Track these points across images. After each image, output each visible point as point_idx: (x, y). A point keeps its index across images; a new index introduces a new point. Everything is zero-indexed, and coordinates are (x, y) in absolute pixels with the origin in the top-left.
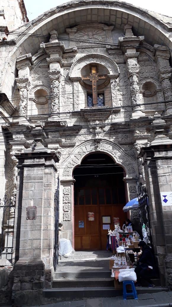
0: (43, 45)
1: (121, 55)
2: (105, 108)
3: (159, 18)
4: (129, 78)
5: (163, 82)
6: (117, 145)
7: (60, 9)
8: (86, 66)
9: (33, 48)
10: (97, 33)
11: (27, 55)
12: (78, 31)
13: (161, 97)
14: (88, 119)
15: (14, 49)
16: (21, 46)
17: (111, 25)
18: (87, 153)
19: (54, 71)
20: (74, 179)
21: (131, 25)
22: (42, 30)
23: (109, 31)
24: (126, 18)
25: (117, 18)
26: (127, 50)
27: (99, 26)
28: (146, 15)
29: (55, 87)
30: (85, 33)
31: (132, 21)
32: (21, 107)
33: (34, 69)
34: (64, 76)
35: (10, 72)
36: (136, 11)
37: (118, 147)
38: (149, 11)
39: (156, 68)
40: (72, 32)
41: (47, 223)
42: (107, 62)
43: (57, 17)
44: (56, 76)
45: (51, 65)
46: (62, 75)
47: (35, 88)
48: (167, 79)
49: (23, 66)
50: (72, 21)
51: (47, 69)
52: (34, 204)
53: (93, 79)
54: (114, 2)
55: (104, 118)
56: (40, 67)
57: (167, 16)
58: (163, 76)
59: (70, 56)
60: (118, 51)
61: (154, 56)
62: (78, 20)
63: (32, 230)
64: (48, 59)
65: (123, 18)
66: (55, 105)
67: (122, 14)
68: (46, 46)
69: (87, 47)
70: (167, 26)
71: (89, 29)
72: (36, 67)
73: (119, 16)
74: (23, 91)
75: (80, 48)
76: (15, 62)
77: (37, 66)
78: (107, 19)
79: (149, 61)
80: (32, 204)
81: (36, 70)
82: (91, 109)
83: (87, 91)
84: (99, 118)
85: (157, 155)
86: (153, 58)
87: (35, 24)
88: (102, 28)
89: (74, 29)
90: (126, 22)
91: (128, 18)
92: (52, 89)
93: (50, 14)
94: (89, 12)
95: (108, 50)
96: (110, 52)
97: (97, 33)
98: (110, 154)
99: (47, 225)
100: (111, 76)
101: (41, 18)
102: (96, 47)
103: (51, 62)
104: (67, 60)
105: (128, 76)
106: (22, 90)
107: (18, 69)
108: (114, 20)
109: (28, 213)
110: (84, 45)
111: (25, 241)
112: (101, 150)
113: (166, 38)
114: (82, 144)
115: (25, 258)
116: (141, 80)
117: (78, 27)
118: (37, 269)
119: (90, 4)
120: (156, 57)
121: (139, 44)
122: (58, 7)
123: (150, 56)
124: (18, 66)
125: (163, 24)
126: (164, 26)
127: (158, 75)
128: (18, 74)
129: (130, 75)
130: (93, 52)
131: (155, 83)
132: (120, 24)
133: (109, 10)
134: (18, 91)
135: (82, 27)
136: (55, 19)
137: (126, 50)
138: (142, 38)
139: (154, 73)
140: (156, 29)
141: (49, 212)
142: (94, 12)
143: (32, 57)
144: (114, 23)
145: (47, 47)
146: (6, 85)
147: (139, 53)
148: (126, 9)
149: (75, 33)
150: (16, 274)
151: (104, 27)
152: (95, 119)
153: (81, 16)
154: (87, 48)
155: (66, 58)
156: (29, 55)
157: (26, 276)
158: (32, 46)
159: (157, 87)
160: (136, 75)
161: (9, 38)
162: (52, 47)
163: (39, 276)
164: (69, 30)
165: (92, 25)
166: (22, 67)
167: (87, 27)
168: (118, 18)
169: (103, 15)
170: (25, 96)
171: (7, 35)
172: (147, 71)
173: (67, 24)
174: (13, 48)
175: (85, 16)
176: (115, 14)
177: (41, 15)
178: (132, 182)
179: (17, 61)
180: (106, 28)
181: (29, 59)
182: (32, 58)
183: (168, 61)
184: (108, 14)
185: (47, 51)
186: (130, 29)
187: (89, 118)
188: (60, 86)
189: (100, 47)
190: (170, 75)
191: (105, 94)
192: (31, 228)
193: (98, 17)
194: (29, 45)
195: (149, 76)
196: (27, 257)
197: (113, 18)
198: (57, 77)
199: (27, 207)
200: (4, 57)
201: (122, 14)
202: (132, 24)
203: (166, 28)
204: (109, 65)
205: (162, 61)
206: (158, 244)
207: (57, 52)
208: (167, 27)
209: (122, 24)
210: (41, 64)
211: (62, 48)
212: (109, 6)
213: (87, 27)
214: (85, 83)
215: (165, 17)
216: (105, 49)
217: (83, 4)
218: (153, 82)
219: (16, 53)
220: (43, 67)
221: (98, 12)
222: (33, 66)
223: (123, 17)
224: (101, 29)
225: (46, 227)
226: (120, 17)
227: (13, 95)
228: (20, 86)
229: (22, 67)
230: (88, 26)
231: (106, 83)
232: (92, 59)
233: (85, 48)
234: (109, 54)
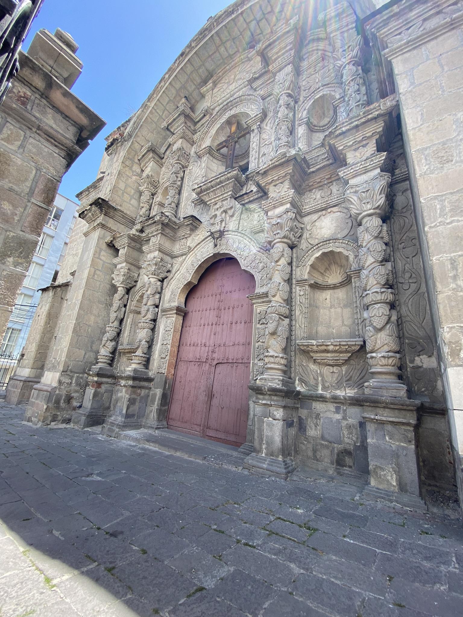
22: (163, 105)
40: (208, 91)
49: (148, 162)
76: (136, 161)
84: (221, 197)
89: (210, 85)
93: (167, 76)
96: (255, 85)
102: (237, 92)
117: (215, 78)
135: (220, 74)
149: (213, 90)
152: (216, 200)
153: (210, 56)
162: (174, 120)
164: (204, 89)
167: (227, 71)
193: (234, 43)
222: (164, 160)
224: (246, 61)
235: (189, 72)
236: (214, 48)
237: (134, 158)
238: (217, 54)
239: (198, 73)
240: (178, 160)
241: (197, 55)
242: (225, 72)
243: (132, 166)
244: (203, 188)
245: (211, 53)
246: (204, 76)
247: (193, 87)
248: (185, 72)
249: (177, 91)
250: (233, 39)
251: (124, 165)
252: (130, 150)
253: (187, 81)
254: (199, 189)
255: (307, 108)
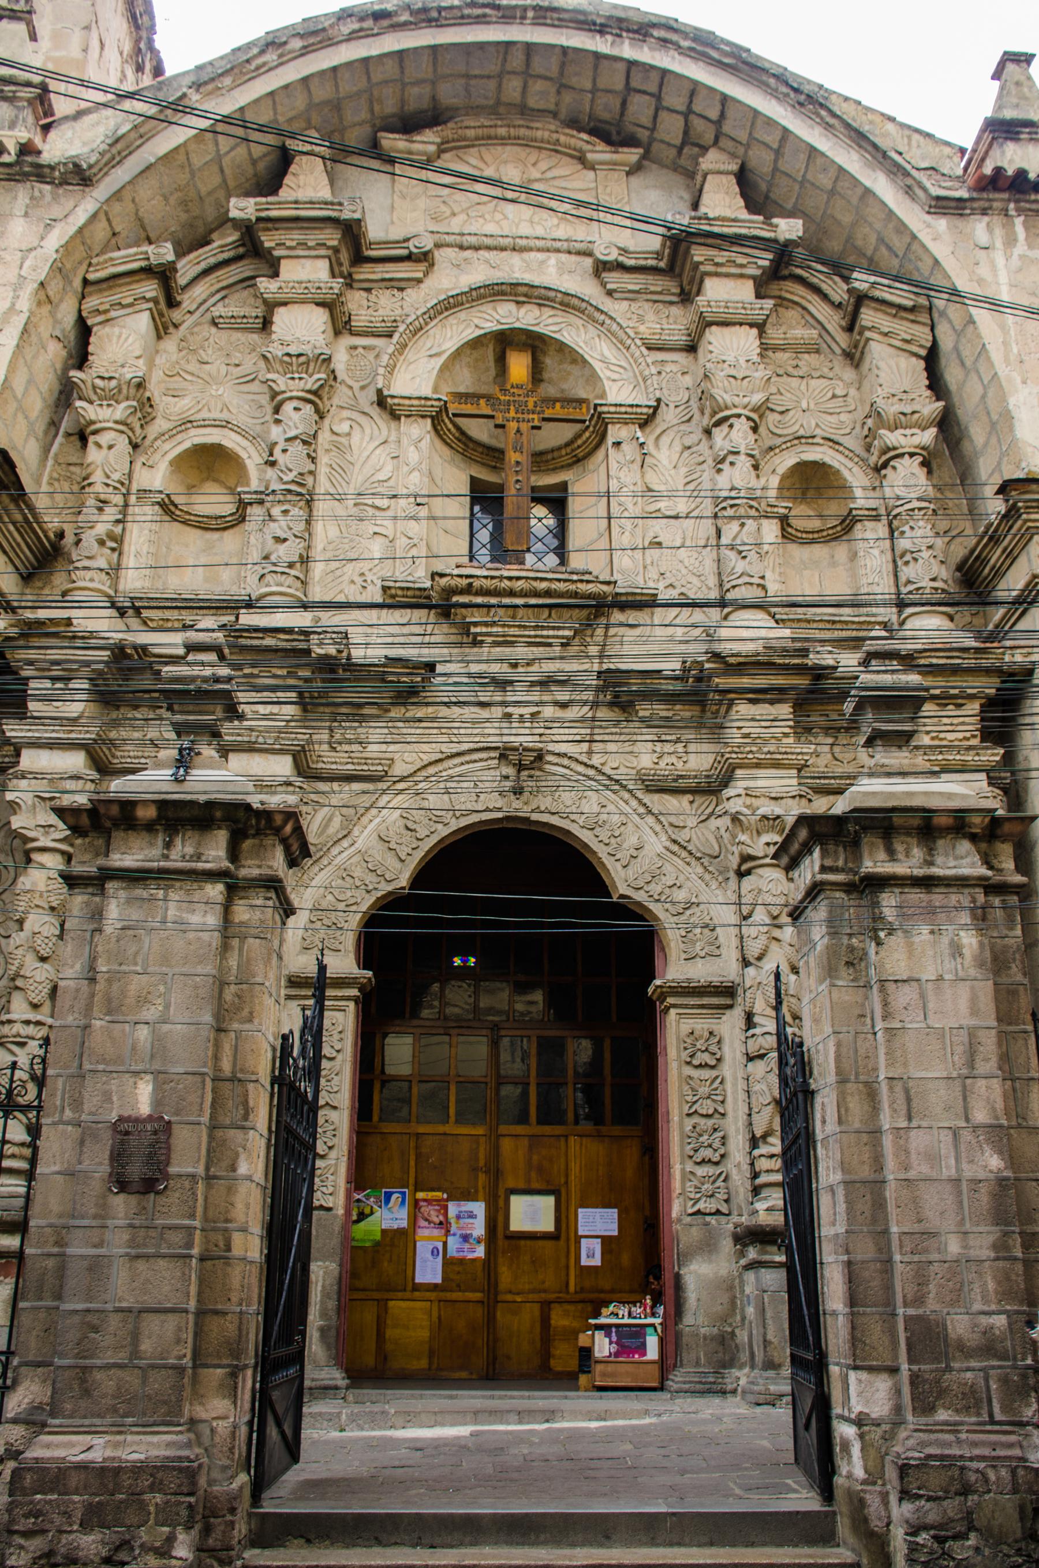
0: (244, 208)
1: (671, 303)
2: (575, 577)
3: (888, 138)
4: (708, 432)
5: (888, 471)
6: (630, 791)
7: (356, 26)
8: (475, 344)
9: (184, 216)
10: (549, 175)
11: (150, 249)
12: (444, 151)
13: (876, 552)
14: (473, 630)
15: (83, 207)
16: (117, 195)
17: (630, 141)
18: (455, 825)
19: (293, 350)
20: (369, 974)
21: (733, 155)
23: (616, 174)
24: (714, 114)
25: (663, 115)
26: (709, 283)
27: (563, 139)
28: (818, 115)
29: (296, 438)
30: (481, 165)
31: (743, 136)
32: (89, 539)
33: (182, 328)
34: (350, 382)
35: (46, 335)
36: (768, 85)
37: (634, 803)
38: (833, 98)
39: (853, 392)
41: (227, 1221)
42: (592, 331)
43: (335, 63)
44: (310, 383)
45: (282, 317)
46: (341, 375)
47: (179, 438)
48: (912, 455)
49: (124, 307)
50: (417, 98)
51: (255, 336)
52: (157, 1102)
53: (512, 414)
54: (654, 26)
55: (561, 633)
56: (216, 324)
57: (928, 136)
58: (892, 438)
59: (391, 280)
60: (657, 283)
61: (850, 328)
62: (449, 94)
63: (138, 1257)
64: (265, 285)
65: (692, 117)
66: (285, 540)
67: (692, 94)
68: (263, 214)
69: (488, 241)
70: (928, 184)
71: (509, 151)
72: (190, 320)
73: (675, 100)
74: (110, 447)
75: (448, 245)
76: (77, 283)
77: (198, 314)
78: (606, 108)
79: (818, 351)
80: (143, 1098)
81: (190, 338)
82: (493, 578)
83: (474, 482)
85: (875, 862)
86: (843, 339)
87: (210, 87)
88: (580, 151)
89: (426, 141)
90: (709, 137)
91: (722, 115)
92: (277, 451)
93: (297, 44)
94: (517, 61)
95: (601, 268)
96: (615, 280)
97: (549, 175)
98: (585, 836)
99: (226, 1230)
100: (612, 409)
101: (248, 61)
102: (539, 250)
103: (285, 304)
104: (372, 298)
105: (706, 421)
106: (104, 439)
107: (89, 322)
108: (646, 120)
109: (118, 1157)
110: (473, 229)
111: (89, 1318)
112: (535, 817)
113: (915, 247)
114: (424, 767)
115: (87, 1422)
116: (771, 449)
117: (448, 131)
118: (152, 1489)
119: (523, 17)
120: (861, 334)
121: (771, 256)
122: (345, 15)
123: (829, 327)
124: (92, 302)
125: (907, 174)
126: (909, 181)
127: (866, 432)
128: (91, 349)
129: (715, 413)
130: (516, 269)
131: (846, 473)
132: (678, 142)
133: (621, 67)
134: (78, 444)
136: (322, 73)
137: (702, 282)
138: (789, 228)
139: (843, 417)
140: (868, 192)
141: (243, 1157)
142: (538, 66)
143: (179, 266)
144: (643, 135)
145: (268, 220)
146: (15, 405)
147: (769, 304)
148: (713, 69)
150: (26, 1516)
151: (589, 147)
153: (468, 76)
154: (489, 248)
155: (368, 290)
156: (166, 252)
157: (86, 1526)
158: (184, 203)
159: (858, 493)
160: (749, 418)
161: (57, 148)
162: (297, 219)
163: (166, 1529)
164: (393, 142)
165: (522, 132)
166: (113, 314)
167: (496, 138)
168: (668, 109)
169: (588, 86)
170: (116, 476)
171: (46, 128)
172: (804, 406)
173: (389, 106)
174: (71, 204)
175: (489, 77)
176: (653, 88)
177: (249, 46)
178: (702, 1007)
179: (91, 277)
180: (599, 152)
181: (164, 275)
182: (176, 270)
183: (922, 364)
184: (619, 85)
185: (268, 240)
186: (728, 173)
187: (476, 624)
188: (324, 437)
189: (558, 251)
190: (928, 436)
191: (574, 506)
192: (132, 1243)
193: (559, 92)
194: (166, 198)
195: (818, 432)
196: (99, 1416)
197: (640, 109)
198: (308, 387)
199: (114, 1117)
200: (16, 246)
201: (692, 94)
202: (741, 150)
203: (920, 193)
204: (607, 353)
205: (892, 363)
206: (859, 1363)
207: (323, 252)
208: (925, 190)
209: (684, 143)
210: (219, 310)
211: (352, 232)
212: (627, 42)
213: (496, 138)
214: (463, 433)
215: (916, 137)
216: (588, 262)
217: (485, 16)
218: (836, 464)
219: (87, 233)
220: (236, 324)
221: (563, 65)
222: (176, 315)
223: (697, 108)
225: (221, 1244)
226: (682, 108)
227: (50, 462)
228: (93, 417)
229: (113, 314)
230: (502, 131)
231: (579, 442)
232: (512, 306)
233: (477, 248)
234: (610, 293)
235: (377, 76)
236: (493, 68)
237: (75, 270)
238: (492, 84)
239: (403, 90)
240: (315, 393)
241: (435, 58)
242: (489, 138)
243: (61, 300)
244: (477, 583)
245: (477, 72)
246: (412, 106)
247: (364, 115)
248: (368, 73)
249: (311, 106)
250: (563, 86)
251: (42, 293)
252: (78, 241)
253: (358, 94)
254: (465, 582)
255: (781, 470)
